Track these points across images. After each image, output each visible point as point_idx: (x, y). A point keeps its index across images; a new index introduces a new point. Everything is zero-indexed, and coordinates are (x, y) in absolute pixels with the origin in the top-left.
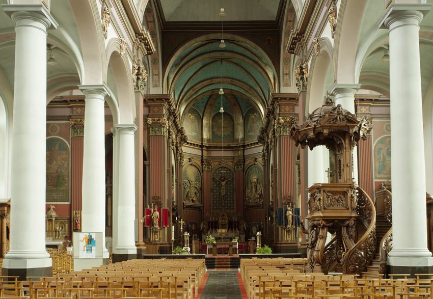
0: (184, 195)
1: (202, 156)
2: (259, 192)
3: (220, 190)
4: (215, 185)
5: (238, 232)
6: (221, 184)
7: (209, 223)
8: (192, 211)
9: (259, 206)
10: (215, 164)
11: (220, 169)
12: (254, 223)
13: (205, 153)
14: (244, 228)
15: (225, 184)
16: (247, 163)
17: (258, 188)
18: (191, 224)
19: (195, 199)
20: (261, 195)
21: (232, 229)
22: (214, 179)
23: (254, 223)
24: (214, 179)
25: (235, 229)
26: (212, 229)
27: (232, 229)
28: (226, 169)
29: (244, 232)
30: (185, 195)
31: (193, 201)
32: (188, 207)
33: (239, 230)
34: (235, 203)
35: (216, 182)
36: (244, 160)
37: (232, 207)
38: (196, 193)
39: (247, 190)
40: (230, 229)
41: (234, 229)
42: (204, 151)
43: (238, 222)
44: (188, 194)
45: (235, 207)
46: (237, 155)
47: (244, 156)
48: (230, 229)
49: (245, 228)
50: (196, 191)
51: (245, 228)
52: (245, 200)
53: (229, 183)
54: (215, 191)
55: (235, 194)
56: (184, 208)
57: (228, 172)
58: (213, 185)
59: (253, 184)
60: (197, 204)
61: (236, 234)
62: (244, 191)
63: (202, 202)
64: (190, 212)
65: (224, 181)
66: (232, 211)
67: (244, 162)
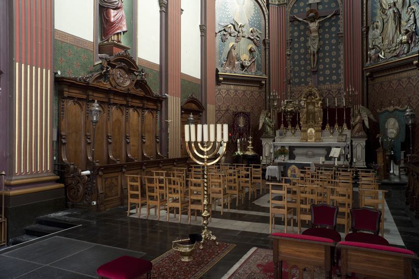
0: (221, 54)
2: (405, 25)
3: (306, 41)
4: (296, 34)
5: (347, 132)
6: (309, 29)
7: (279, 115)
8: (242, 88)
12: (391, 108)
15: (319, 28)
17: (405, 16)
18: (236, 115)
19: (247, 64)
20: (410, 35)
21: (332, 125)
22: (293, 20)
23: (391, 108)
24: (293, 20)
25: (341, 125)
26: (286, 126)
27: (332, 125)
29: (362, 133)
30: (225, 56)
31: (243, 67)
32: (229, 79)
33: (349, 127)
34: (342, 67)
35: (298, 26)
38: (251, 51)
39: (371, 33)
40: (328, 126)
41: (336, 126)
43: (348, 110)
44: (230, 52)
45: (342, 77)
48: (328, 126)
49: (367, 123)
50: (254, 47)
51: (367, 123)
52: (365, 57)
53: (327, 24)
54: (296, 45)
55: (341, 47)
56: (218, 82)
58: (292, 32)
59: (390, 12)
60: (251, 74)
62: (365, 35)
63: (267, 71)
64: (236, 91)
65: (313, 20)
66: (334, 86)
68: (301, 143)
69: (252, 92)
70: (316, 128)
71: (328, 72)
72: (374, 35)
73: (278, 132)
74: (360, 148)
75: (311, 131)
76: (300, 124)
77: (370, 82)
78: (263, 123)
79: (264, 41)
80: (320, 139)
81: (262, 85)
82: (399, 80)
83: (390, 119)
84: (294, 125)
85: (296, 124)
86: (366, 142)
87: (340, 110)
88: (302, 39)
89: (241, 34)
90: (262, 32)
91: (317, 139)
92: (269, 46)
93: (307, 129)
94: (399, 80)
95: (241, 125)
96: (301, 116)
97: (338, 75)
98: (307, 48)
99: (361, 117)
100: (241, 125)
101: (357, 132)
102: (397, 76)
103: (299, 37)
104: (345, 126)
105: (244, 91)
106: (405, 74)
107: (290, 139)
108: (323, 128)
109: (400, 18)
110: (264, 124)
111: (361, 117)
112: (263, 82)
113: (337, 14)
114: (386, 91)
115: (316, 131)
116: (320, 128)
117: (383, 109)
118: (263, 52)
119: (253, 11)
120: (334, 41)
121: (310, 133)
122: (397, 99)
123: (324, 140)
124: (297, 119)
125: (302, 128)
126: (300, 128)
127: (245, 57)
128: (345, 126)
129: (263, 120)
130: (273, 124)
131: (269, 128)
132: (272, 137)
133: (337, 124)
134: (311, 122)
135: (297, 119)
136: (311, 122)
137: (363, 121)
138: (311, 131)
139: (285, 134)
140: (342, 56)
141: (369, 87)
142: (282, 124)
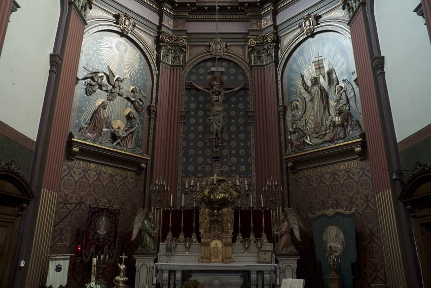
1: (159, 27)
3: (206, 116)
4: (193, 106)
5: (269, 247)
7: (166, 214)
8: (110, 170)
9: (345, 153)
10: (194, 53)
11: (209, 64)
13: (168, 23)
14: (291, 232)
16: (285, 42)
18: (95, 212)
19: (121, 133)
21: (246, 236)
22: (190, 88)
23: (330, 212)
24: (190, 88)
25: (258, 236)
26: (176, 235)
27: (246, 236)
28: (225, 64)
29: (292, 249)
30: (87, 116)
31: (114, 137)
32: (89, 153)
33: (271, 239)
34: (253, 154)
36: (276, 34)
37: (243, 168)
40: (240, 237)
41: (252, 237)
42: (165, 17)
43: (267, 214)
44: (95, 112)
45: (253, 167)
46: (255, 28)
47: (276, 27)
48: (240, 237)
49: (297, 233)
51: (297, 233)
54: (192, 121)
56: (70, 155)
57: (232, 71)
61: (262, 255)
63: (150, 148)
64: (99, 173)
67: (277, 41)
68: (201, 264)
69: (124, 178)
70: (223, 240)
71: (234, 160)
72: (294, 116)
73: (163, 246)
74: (291, 272)
75: (216, 244)
76: (198, 234)
77: (292, 176)
78: (140, 229)
79: (149, 107)
80: (231, 258)
81: (141, 169)
82: (334, 174)
83: (330, 227)
84: (188, 235)
85: (192, 232)
86: (298, 262)
87: (257, 214)
88: (201, 113)
89: (117, 90)
90: (148, 95)
91: (225, 258)
92: (155, 115)
93: (211, 241)
94: (334, 174)
95: (102, 232)
96: (201, 220)
97: (248, 165)
98: (207, 126)
99: (289, 224)
100: (102, 232)
101: (284, 247)
102: (330, 168)
103: (197, 109)
104: (264, 236)
105: (112, 176)
106: (342, 166)
107: (183, 258)
108: (234, 240)
109: (327, 97)
110: (140, 231)
111: (289, 224)
112: (144, 165)
113: (245, 89)
114: (315, 189)
115: (225, 245)
116: (230, 240)
117: (318, 214)
118: (146, 123)
119: (137, 66)
120: (241, 121)
121: (214, 248)
122: (348, 198)
123: (236, 259)
124: (194, 225)
125: (202, 240)
126: (199, 239)
127: (119, 124)
128: (264, 236)
129: (140, 224)
130: (155, 231)
131: (148, 239)
132: (152, 254)
133: (252, 233)
134: (216, 231)
135: (194, 225)
136: (216, 231)
137: (292, 230)
138: (216, 244)
139: (174, 248)
140: (253, 140)
141: (291, 182)
142: (170, 233)
